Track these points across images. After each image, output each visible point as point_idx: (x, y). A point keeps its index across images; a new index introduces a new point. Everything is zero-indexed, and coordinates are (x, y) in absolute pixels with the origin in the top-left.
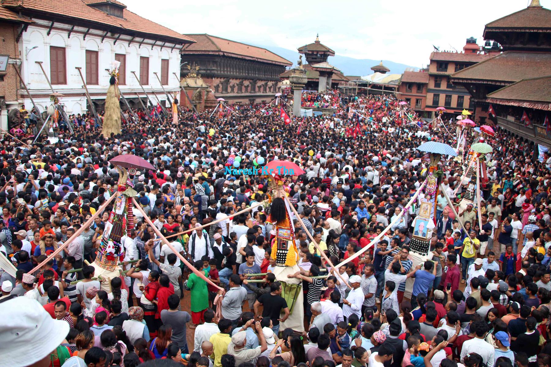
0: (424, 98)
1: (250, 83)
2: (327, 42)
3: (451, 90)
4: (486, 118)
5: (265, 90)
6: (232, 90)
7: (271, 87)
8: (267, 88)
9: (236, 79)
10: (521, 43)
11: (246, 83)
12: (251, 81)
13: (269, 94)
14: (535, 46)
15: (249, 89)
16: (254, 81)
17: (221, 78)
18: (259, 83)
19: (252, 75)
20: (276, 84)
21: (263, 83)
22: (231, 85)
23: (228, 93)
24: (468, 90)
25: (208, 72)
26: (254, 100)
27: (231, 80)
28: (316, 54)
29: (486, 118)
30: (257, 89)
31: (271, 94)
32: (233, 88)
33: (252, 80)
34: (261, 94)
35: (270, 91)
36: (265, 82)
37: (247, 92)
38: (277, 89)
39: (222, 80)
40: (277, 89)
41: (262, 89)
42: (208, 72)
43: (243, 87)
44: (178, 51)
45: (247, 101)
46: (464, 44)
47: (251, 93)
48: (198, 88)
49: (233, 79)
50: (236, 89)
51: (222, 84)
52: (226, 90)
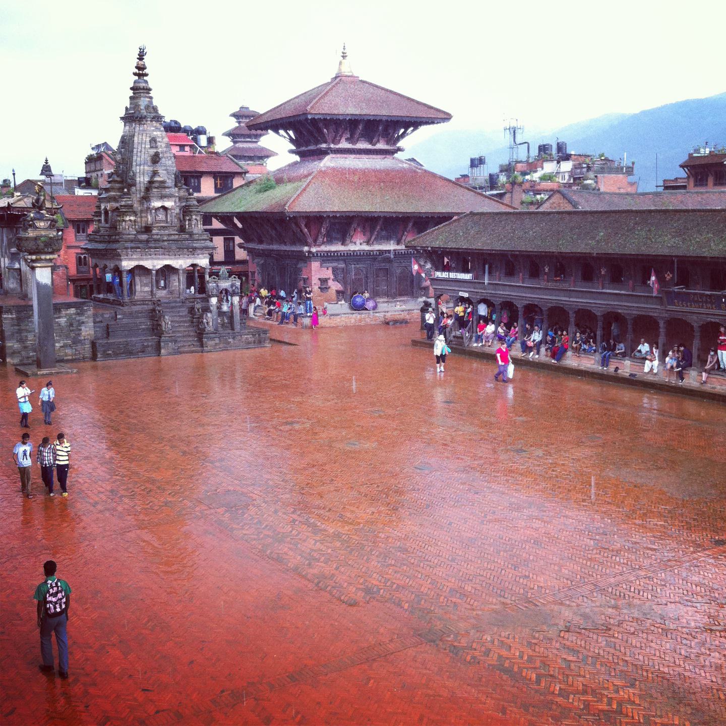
4: (329, 279)
10: (350, 140)
14: (369, 147)
29: (329, 279)
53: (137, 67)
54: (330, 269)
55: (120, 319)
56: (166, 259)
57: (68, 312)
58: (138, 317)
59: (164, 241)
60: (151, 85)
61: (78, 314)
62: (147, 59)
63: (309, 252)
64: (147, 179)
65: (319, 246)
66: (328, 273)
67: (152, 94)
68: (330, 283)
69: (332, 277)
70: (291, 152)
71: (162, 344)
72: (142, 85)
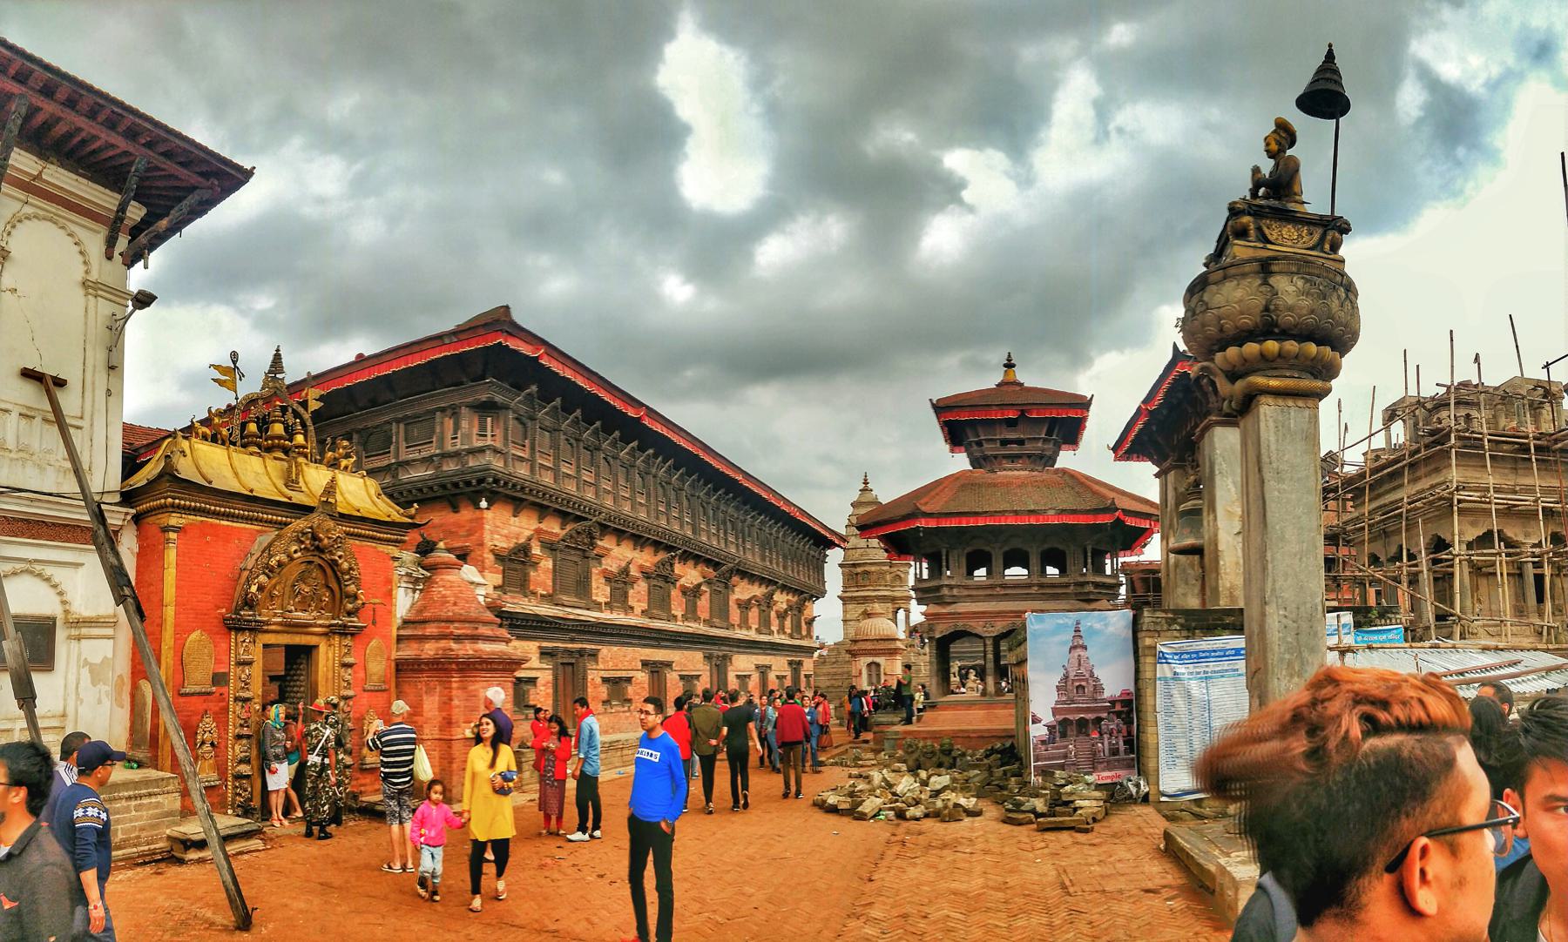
6: (619, 598)
8: (773, 614)
9: (639, 540)
11: (690, 575)
13: (777, 638)
15: (704, 602)
16: (724, 572)
17: (542, 511)
18: (744, 591)
19: (709, 538)
20: (800, 608)
21: (758, 591)
22: (612, 565)
23: (598, 606)
26: (726, 659)
27: (606, 543)
33: (716, 566)
34: (752, 635)
35: (782, 630)
37: (696, 619)
39: (553, 527)
41: (754, 614)
49: (620, 535)
50: (639, 594)
51: (550, 547)
52: (582, 587)
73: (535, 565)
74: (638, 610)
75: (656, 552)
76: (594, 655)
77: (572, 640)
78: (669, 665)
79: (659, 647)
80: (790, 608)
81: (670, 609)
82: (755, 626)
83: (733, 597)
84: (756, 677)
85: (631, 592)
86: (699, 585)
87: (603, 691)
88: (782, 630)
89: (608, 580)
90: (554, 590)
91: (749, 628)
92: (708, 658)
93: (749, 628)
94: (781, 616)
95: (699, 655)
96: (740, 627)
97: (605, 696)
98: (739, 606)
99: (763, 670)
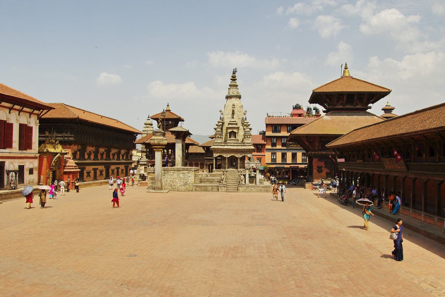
0: (263, 157)
1: (105, 151)
2: (177, 112)
3: (285, 148)
4: (323, 167)
5: (118, 159)
6: (89, 158)
7: (124, 154)
8: (121, 155)
9: (92, 146)
11: (102, 150)
12: (106, 149)
22: (88, 151)
23: (85, 159)
24: (301, 145)
25: (66, 139)
28: (168, 122)
30: (111, 157)
31: (124, 161)
32: (89, 155)
35: (123, 159)
36: (118, 150)
38: (129, 157)
40: (129, 157)
42: (66, 139)
43: (99, 155)
44: (36, 117)
45: (101, 168)
46: (291, 111)
47: (106, 160)
48: (57, 153)
50: (92, 157)
53: (232, 77)
54: (323, 162)
55: (209, 177)
56: (233, 153)
57: (183, 172)
58: (216, 177)
59: (231, 146)
60: (237, 84)
61: (188, 173)
62: (237, 74)
63: (311, 154)
64: (229, 120)
65: (317, 151)
66: (323, 164)
67: (238, 87)
68: (323, 168)
69: (324, 166)
70: (324, 112)
71: (219, 187)
72: (232, 84)
73: (77, 154)
74: (92, 159)
75: (95, 147)
76: (85, 168)
77: (82, 166)
78: (97, 169)
79: (95, 165)
80: (125, 153)
81: (98, 158)
82: (116, 159)
83: (111, 153)
84: (116, 171)
85: (91, 156)
86: (104, 152)
87: (86, 174)
88: (123, 159)
89: (88, 154)
90: (80, 157)
91: (115, 159)
92: (105, 167)
93: (115, 159)
94: (123, 156)
95: (103, 166)
96: (112, 159)
97: (86, 175)
98: (112, 155)
99: (118, 169)
